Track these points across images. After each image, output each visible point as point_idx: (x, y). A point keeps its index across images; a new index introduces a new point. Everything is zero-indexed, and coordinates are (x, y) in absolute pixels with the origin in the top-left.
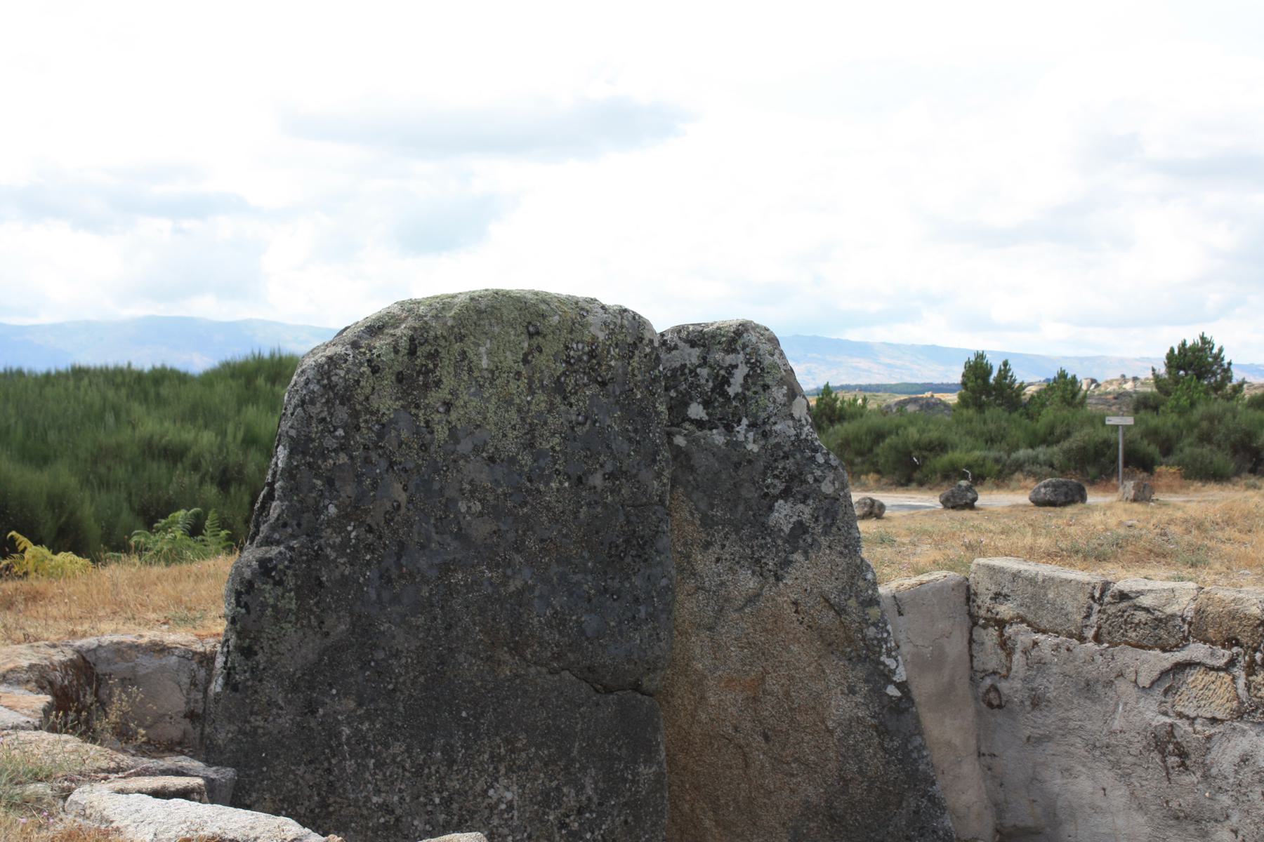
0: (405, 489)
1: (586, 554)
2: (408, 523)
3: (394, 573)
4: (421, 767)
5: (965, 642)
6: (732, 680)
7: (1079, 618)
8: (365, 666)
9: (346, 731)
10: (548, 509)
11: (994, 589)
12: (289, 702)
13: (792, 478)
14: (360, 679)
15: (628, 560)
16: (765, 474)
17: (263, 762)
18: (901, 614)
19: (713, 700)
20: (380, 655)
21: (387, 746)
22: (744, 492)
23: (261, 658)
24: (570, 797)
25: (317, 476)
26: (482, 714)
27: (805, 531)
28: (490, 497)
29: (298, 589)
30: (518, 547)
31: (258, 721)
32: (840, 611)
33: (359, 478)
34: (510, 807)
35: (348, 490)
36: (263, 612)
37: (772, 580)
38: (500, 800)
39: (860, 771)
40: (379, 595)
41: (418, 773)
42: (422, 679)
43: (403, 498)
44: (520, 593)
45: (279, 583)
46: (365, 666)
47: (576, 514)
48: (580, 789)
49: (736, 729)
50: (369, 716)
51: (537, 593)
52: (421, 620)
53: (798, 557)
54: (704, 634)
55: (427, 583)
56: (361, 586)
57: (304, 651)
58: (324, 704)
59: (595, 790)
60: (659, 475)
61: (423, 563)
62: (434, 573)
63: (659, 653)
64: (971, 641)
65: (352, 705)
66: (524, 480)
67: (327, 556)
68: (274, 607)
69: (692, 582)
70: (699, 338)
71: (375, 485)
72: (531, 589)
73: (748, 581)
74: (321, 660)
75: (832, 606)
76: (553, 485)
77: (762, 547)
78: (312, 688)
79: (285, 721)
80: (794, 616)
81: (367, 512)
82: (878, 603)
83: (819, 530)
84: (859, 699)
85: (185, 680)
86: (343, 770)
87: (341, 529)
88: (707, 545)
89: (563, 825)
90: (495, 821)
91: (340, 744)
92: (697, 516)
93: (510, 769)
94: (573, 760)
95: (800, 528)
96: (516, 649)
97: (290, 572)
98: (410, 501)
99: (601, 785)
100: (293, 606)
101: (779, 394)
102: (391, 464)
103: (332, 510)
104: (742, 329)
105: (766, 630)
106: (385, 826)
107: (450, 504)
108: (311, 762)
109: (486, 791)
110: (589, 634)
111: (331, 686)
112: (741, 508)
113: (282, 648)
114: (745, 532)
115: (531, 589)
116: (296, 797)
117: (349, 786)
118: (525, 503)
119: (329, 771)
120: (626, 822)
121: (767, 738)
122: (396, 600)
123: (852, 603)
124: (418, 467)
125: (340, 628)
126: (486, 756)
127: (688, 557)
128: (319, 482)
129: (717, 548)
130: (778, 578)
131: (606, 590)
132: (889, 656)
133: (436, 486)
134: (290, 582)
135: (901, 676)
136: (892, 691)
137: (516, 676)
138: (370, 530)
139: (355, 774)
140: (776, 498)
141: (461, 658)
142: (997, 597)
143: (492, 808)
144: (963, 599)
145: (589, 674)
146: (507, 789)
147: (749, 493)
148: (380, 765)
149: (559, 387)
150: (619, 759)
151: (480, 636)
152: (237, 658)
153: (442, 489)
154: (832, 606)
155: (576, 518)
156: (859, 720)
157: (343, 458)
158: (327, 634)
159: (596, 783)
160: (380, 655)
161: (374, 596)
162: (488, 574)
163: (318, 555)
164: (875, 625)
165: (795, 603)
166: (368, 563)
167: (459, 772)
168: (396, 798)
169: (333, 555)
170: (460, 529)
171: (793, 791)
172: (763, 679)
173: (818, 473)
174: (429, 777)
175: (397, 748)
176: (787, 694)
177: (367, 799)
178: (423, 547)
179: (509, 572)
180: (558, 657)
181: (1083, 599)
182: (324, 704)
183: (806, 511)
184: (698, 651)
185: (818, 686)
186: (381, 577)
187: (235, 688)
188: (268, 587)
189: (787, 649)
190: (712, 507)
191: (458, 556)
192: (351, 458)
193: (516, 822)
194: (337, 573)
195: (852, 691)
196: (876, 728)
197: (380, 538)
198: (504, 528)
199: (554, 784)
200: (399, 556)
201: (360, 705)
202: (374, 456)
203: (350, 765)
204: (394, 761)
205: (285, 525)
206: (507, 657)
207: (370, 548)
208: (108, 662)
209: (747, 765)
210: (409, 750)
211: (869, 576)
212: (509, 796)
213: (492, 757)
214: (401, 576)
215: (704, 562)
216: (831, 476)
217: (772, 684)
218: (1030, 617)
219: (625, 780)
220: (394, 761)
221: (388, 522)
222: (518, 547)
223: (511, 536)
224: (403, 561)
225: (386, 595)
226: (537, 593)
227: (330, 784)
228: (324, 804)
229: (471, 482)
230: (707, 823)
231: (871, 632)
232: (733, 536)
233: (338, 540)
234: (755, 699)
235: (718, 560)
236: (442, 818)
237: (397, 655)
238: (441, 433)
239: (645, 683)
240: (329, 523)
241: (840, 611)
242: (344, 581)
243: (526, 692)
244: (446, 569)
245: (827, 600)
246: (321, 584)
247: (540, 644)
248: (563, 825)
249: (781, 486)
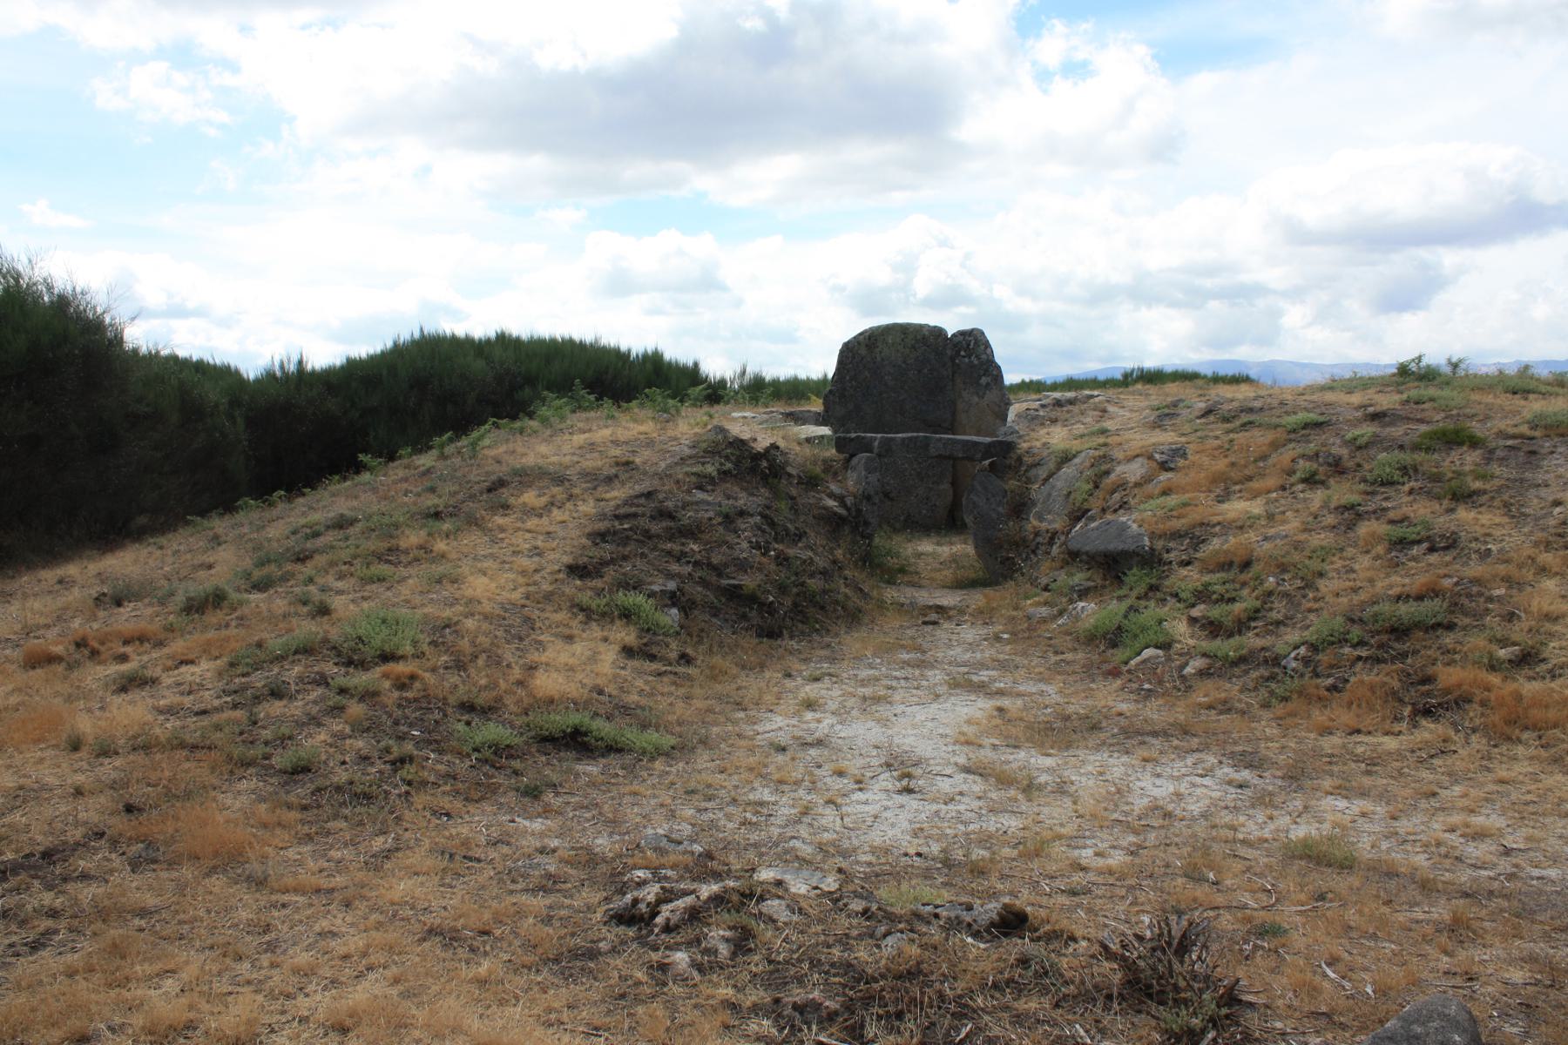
70: (962, 333)
73: (976, 399)
95: (988, 384)
101: (982, 347)
104: (973, 330)
149: (913, 347)
183: (989, 379)
215: (965, 394)
238: (879, 359)
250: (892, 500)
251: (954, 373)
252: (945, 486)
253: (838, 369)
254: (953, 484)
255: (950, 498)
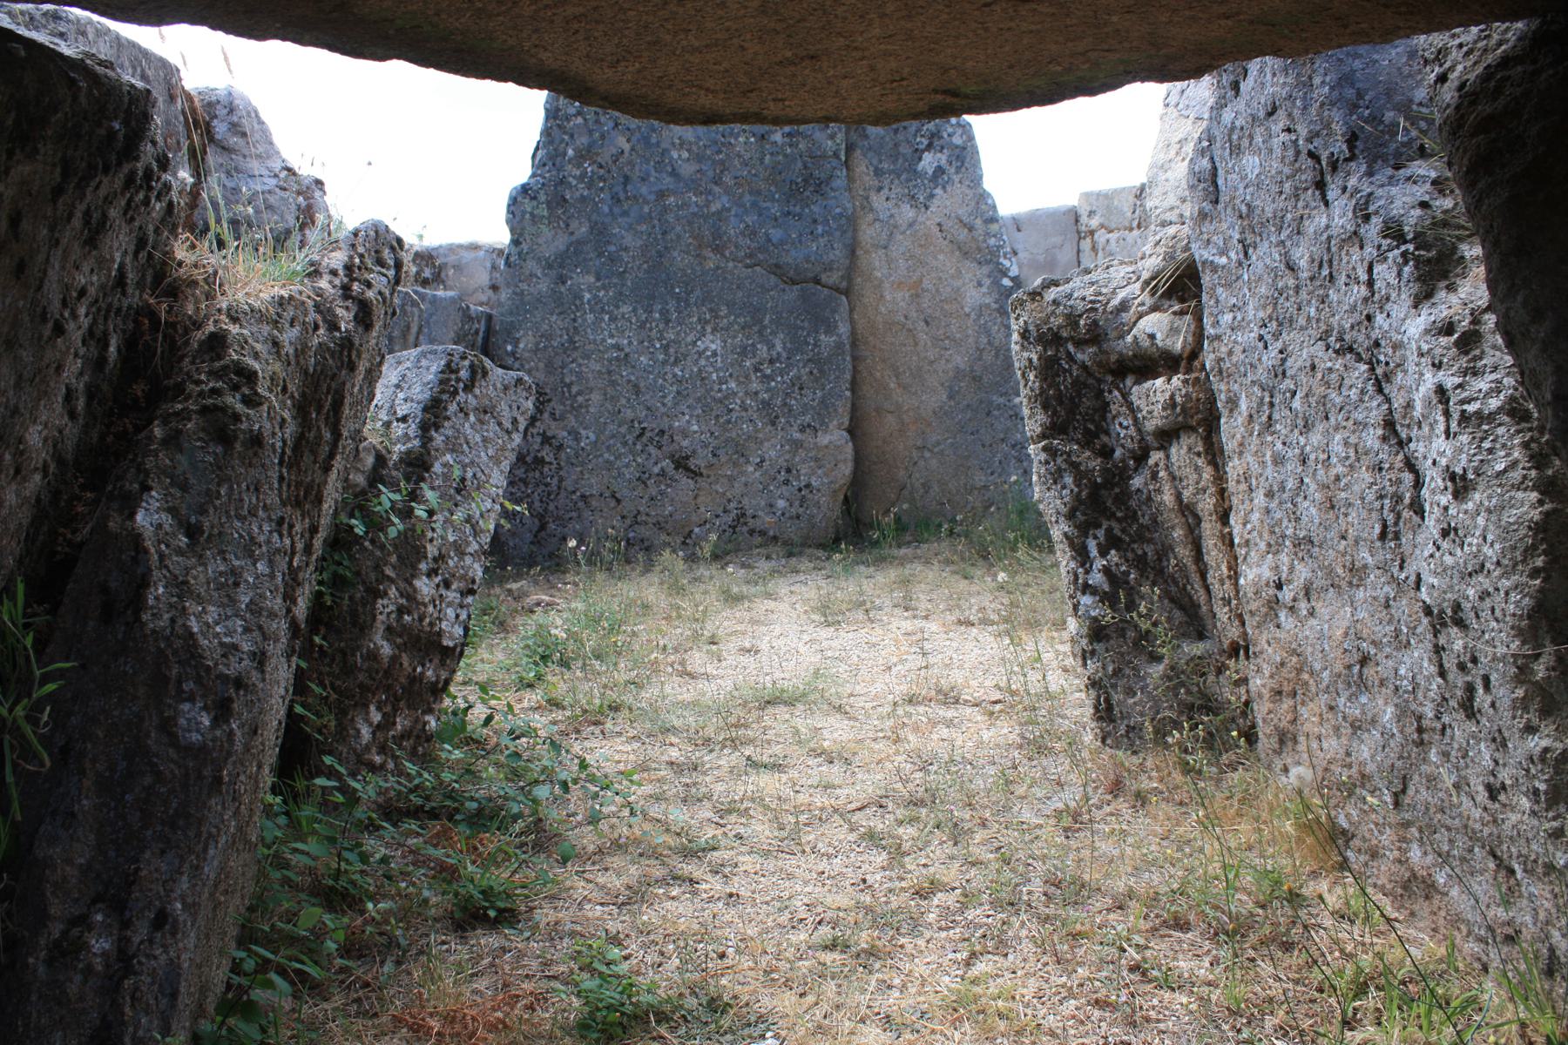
0: (628, 141)
1: (772, 188)
2: (631, 163)
3: (622, 196)
4: (644, 323)
5: (1075, 251)
6: (901, 283)
7: (1129, 214)
8: (600, 255)
9: (587, 296)
10: (739, 156)
11: (1088, 209)
12: (546, 275)
13: (933, 135)
14: (597, 263)
15: (807, 193)
16: (915, 135)
17: (527, 311)
18: (1019, 230)
19: (888, 297)
20: (612, 248)
21: (617, 307)
22: (901, 149)
23: (525, 247)
24: (763, 350)
25: (565, 133)
26: (692, 291)
27: (944, 173)
28: (694, 148)
29: (548, 203)
30: (717, 181)
31: (524, 286)
32: (971, 229)
33: (591, 132)
34: (715, 354)
35: (583, 140)
36: (523, 216)
37: (923, 210)
38: (706, 349)
39: (989, 343)
40: (611, 210)
41: (642, 326)
42: (645, 266)
43: (627, 147)
44: (719, 212)
45: (534, 198)
46: (600, 255)
47: (762, 160)
48: (771, 346)
49: (906, 317)
50: (604, 287)
51: (733, 213)
52: (644, 228)
53: (938, 191)
54: (881, 252)
55: (648, 203)
56: (596, 204)
57: (556, 243)
58: (571, 278)
59: (784, 348)
60: (832, 137)
61: (644, 190)
62: (653, 197)
63: (832, 257)
64: (1079, 251)
65: (592, 280)
66: (719, 136)
67: (570, 183)
68: (532, 214)
69: (871, 217)
71: (603, 137)
72: (729, 210)
73: (907, 212)
74: (568, 249)
75: (965, 225)
76: (741, 139)
77: (915, 186)
78: (562, 266)
79: (543, 286)
80: (939, 234)
81: (598, 154)
82: (997, 221)
83: (953, 170)
84: (984, 290)
85: (489, 265)
86: (585, 320)
87: (579, 166)
88: (880, 189)
89: (757, 370)
90: (703, 362)
91: (583, 304)
92: (872, 169)
93: (714, 330)
94: (765, 327)
95: (940, 171)
96: (718, 250)
97: (542, 192)
98: (632, 149)
99: (788, 345)
100: (545, 213)
102: (617, 125)
103: (570, 152)
105: (921, 246)
106: (617, 359)
107: (665, 152)
108: (561, 313)
109: (695, 342)
110: (775, 240)
111: (576, 266)
112: (900, 161)
113: (540, 241)
114: (904, 177)
115: (729, 210)
116: (551, 335)
117: (589, 331)
118: (721, 152)
119: (574, 320)
120: (811, 373)
121: (927, 323)
122: (625, 214)
123: (979, 222)
124: (639, 128)
125: (583, 230)
126: (695, 319)
127: (867, 198)
128: (566, 137)
129: (886, 191)
130: (927, 208)
131: (789, 213)
132: (1005, 258)
133: (654, 141)
134: (542, 198)
135: (1014, 272)
136: (1006, 282)
137: (718, 268)
138: (601, 167)
139: (594, 323)
140: (923, 151)
141: (675, 254)
142: (1091, 213)
143: (700, 354)
144: (1073, 221)
145: (777, 269)
146: (713, 342)
147: (905, 150)
148: (613, 319)
150: (803, 328)
151: (690, 240)
152: (513, 248)
153: (658, 142)
154: (965, 225)
155: (762, 163)
156: (988, 306)
157: (579, 120)
158: (572, 233)
159: (784, 344)
160: (612, 248)
161: (606, 209)
162: (694, 199)
163: (562, 182)
164: (995, 236)
165: (939, 225)
166: (602, 189)
167: (673, 328)
168: (626, 342)
169: (574, 182)
170: (674, 170)
171: (947, 361)
172: (921, 281)
173: (950, 130)
174: (651, 329)
175: (626, 309)
176: (937, 290)
177: (604, 340)
178: (643, 179)
179: (710, 198)
180: (751, 256)
181: (1132, 199)
182: (571, 278)
183: (943, 158)
184: (877, 263)
185: (959, 283)
186: (612, 198)
187: (510, 266)
188: (527, 201)
189: (936, 259)
190: (881, 162)
191: (671, 187)
192: (585, 119)
193: (719, 365)
194: (578, 194)
195: (980, 284)
196: (998, 310)
197: (609, 172)
198: (704, 168)
199: (750, 342)
200: (625, 184)
201: (598, 279)
202: (603, 119)
203: (590, 317)
204: (623, 317)
205: (544, 165)
206: (711, 255)
207: (602, 178)
208: (446, 256)
209: (916, 344)
210: (634, 310)
211: (990, 202)
212: (713, 347)
213: (699, 320)
214: (628, 198)
215: (878, 201)
216: (960, 131)
217: (926, 284)
218: (1106, 223)
219: (808, 344)
220: (623, 317)
221: (615, 162)
222: (717, 181)
223: (710, 174)
224: (629, 188)
225: (616, 210)
226: (733, 213)
227: (575, 328)
228: (571, 341)
229: (680, 138)
230: (892, 385)
231: (992, 241)
232: (896, 182)
233: (578, 173)
234: (917, 296)
235: (887, 199)
236: (661, 357)
237: (626, 249)
239: (824, 278)
240: (570, 161)
241: (971, 229)
242: (583, 199)
243: (725, 278)
244: (661, 195)
245: (961, 221)
246: (565, 200)
247: (736, 247)
248: (757, 370)
249: (926, 142)
250: (695, 474)
251: (850, 149)
252: (834, 436)
253: (546, 132)
254: (851, 431)
255: (847, 469)
